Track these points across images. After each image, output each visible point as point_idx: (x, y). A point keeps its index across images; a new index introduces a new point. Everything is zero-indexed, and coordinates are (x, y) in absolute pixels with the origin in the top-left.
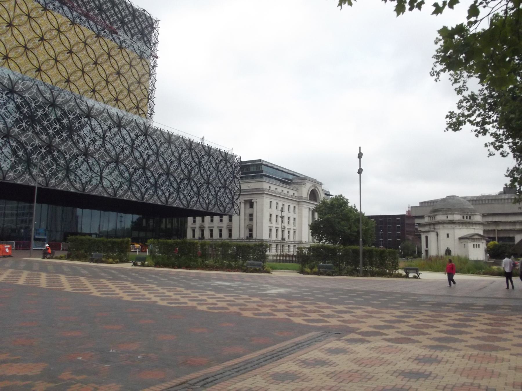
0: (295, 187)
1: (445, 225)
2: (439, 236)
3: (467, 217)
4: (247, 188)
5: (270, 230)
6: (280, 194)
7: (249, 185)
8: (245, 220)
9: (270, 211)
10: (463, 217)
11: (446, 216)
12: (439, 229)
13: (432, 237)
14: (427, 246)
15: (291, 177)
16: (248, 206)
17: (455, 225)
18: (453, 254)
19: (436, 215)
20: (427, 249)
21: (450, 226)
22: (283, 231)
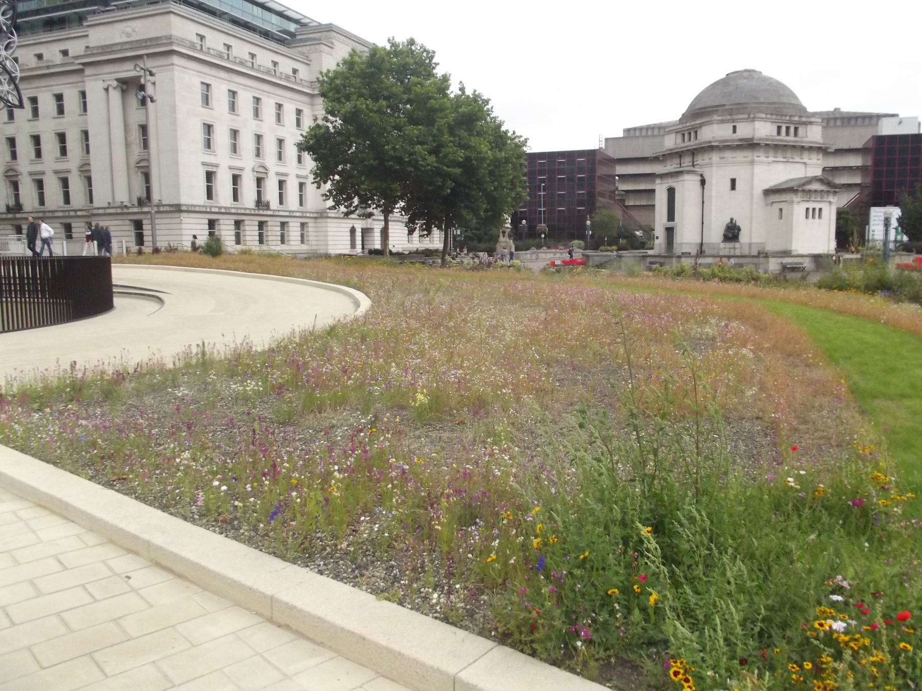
0: (303, 54)
1: (728, 154)
2: (706, 186)
3: (788, 128)
4: (125, 39)
5: (210, 176)
6: (242, 63)
7: (129, 27)
8: (127, 145)
9: (206, 115)
10: (779, 128)
11: (730, 126)
12: (710, 165)
13: (687, 188)
14: (671, 216)
15: (292, 27)
16: (133, 102)
17: (756, 154)
18: (744, 237)
19: (701, 126)
20: (670, 224)
21: (740, 156)
22: (259, 181)
